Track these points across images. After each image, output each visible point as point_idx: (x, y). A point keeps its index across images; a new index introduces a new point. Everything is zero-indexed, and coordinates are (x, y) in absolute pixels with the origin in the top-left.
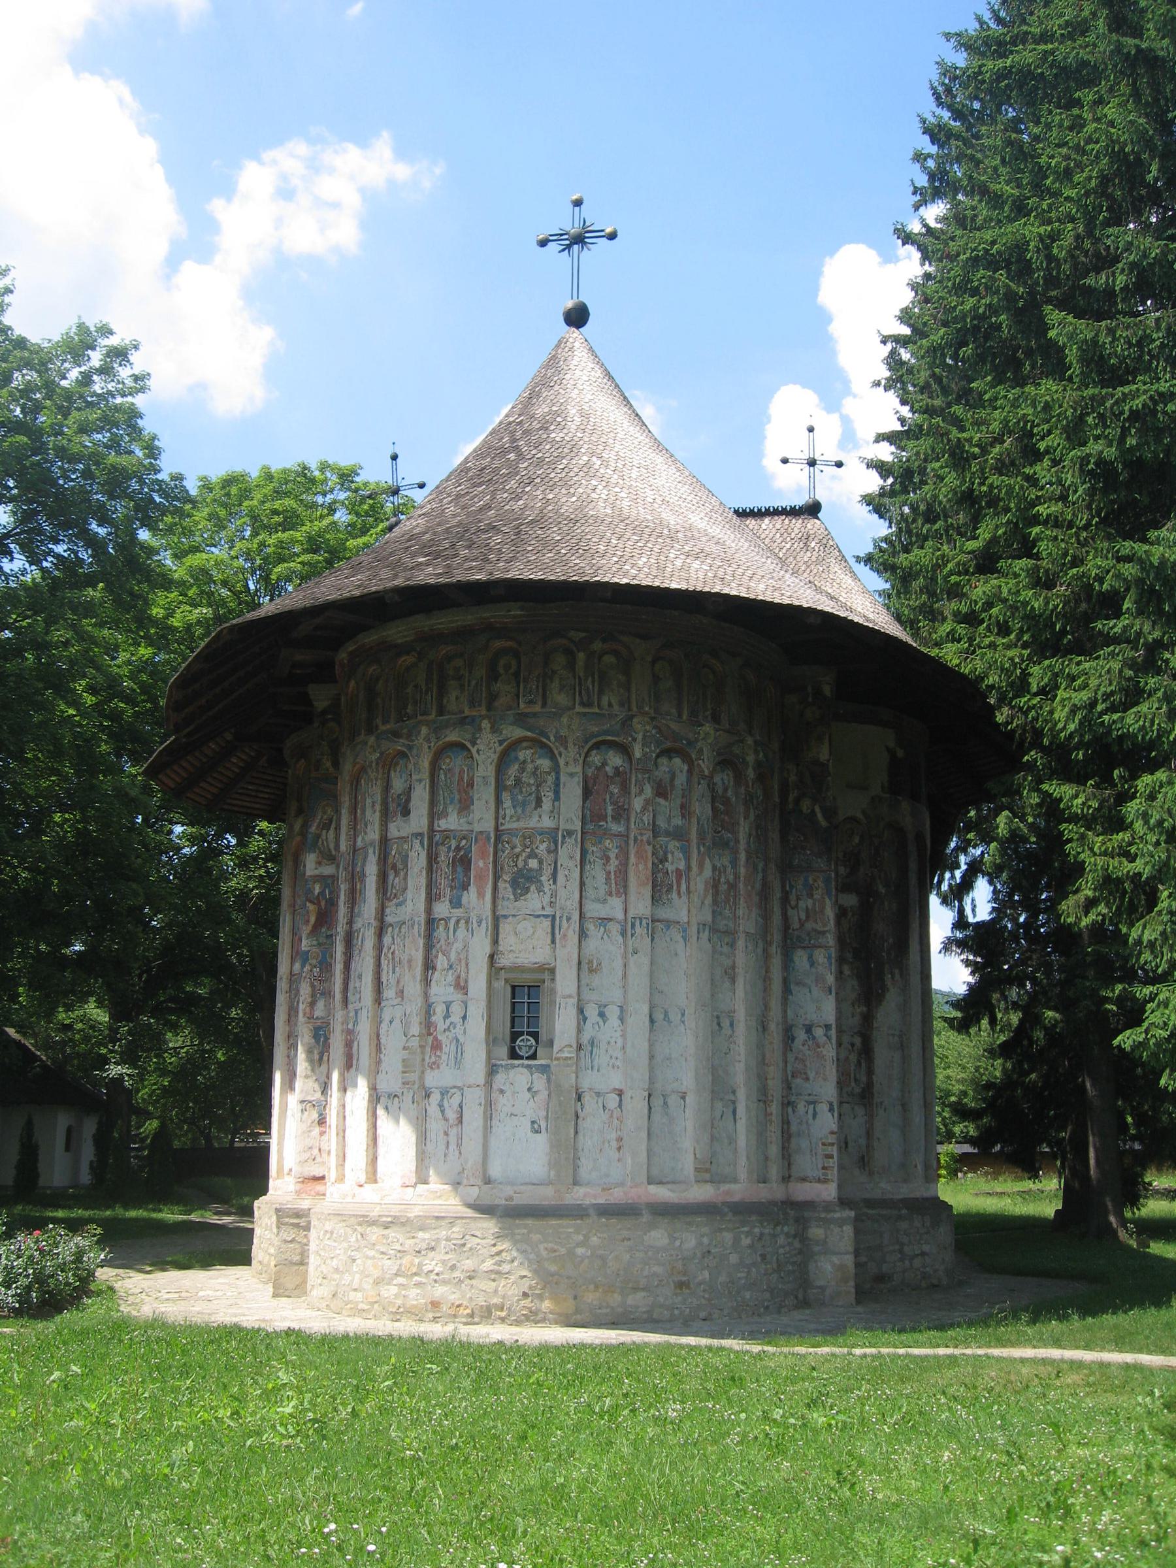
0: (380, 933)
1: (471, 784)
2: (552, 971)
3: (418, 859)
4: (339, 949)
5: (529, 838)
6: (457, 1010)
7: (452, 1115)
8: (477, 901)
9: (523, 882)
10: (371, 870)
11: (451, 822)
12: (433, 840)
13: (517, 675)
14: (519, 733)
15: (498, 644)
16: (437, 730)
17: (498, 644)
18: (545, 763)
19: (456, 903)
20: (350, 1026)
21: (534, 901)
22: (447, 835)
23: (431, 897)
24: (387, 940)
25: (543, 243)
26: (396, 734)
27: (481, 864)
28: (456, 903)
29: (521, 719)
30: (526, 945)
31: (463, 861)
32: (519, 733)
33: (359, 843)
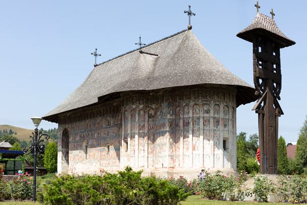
0: (204, 130)
1: (219, 110)
2: (228, 138)
3: (212, 121)
4: (191, 132)
5: (226, 119)
6: (218, 143)
7: (218, 158)
8: (221, 127)
9: (225, 126)
10: (201, 120)
11: (216, 116)
12: (214, 118)
13: (224, 96)
14: (225, 104)
15: (223, 91)
16: (214, 102)
17: (223, 91)
18: (227, 109)
19: (217, 128)
20: (194, 144)
21: (226, 129)
22: (215, 118)
23: (214, 126)
24: (205, 132)
25: (185, 12)
26: (207, 101)
27: (220, 123)
28: (217, 128)
29: (226, 102)
30: (226, 136)
31: (218, 122)
32: (225, 104)
33: (194, 116)
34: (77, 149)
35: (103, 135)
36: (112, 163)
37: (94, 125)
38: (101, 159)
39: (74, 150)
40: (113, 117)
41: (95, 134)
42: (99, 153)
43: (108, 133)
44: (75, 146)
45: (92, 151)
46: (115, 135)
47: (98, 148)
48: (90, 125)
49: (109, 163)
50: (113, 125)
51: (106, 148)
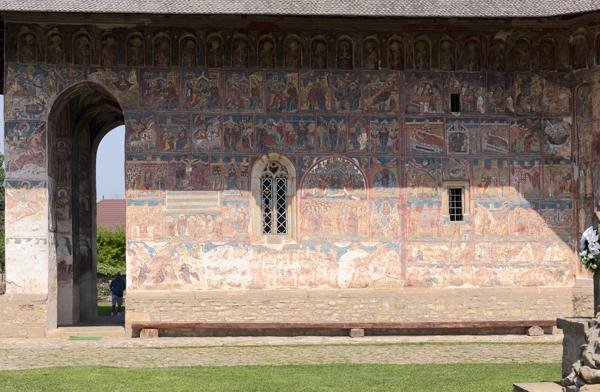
34: (201, 183)
35: (413, 141)
36: (492, 252)
37: (355, 98)
38: (407, 233)
39: (178, 188)
40: (489, 82)
41: (354, 136)
42: (395, 215)
43: (457, 142)
44: (181, 174)
45: (302, 204)
46: (504, 150)
47: (396, 191)
48: (318, 96)
49: (468, 255)
50: (490, 110)
51: (444, 196)
